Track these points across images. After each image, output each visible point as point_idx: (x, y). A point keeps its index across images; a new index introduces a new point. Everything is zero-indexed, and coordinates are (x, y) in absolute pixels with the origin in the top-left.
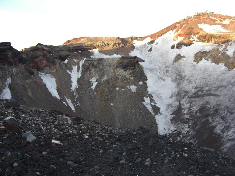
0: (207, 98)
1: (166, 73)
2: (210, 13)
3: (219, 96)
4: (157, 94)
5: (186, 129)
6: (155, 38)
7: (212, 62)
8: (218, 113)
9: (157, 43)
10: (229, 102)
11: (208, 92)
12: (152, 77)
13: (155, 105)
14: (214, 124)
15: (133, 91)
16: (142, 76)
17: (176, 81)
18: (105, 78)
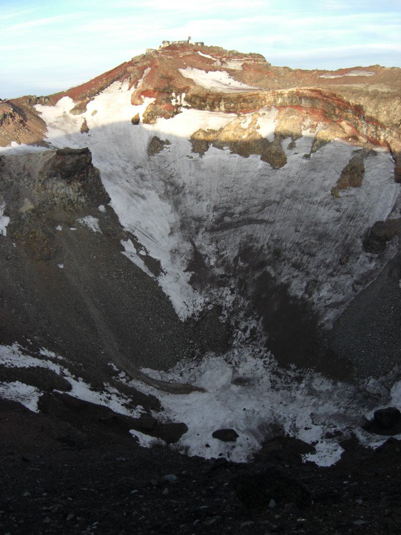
0: (247, 229)
1: (140, 181)
2: (197, 43)
3: (272, 223)
4: (141, 230)
5: (229, 299)
6: (84, 98)
7: (231, 153)
8: (282, 257)
9: (95, 112)
10: (297, 233)
11: (246, 217)
12: (117, 192)
13: (147, 255)
14: (283, 280)
15: (95, 230)
16: (101, 193)
17: (169, 199)
18: (27, 206)
